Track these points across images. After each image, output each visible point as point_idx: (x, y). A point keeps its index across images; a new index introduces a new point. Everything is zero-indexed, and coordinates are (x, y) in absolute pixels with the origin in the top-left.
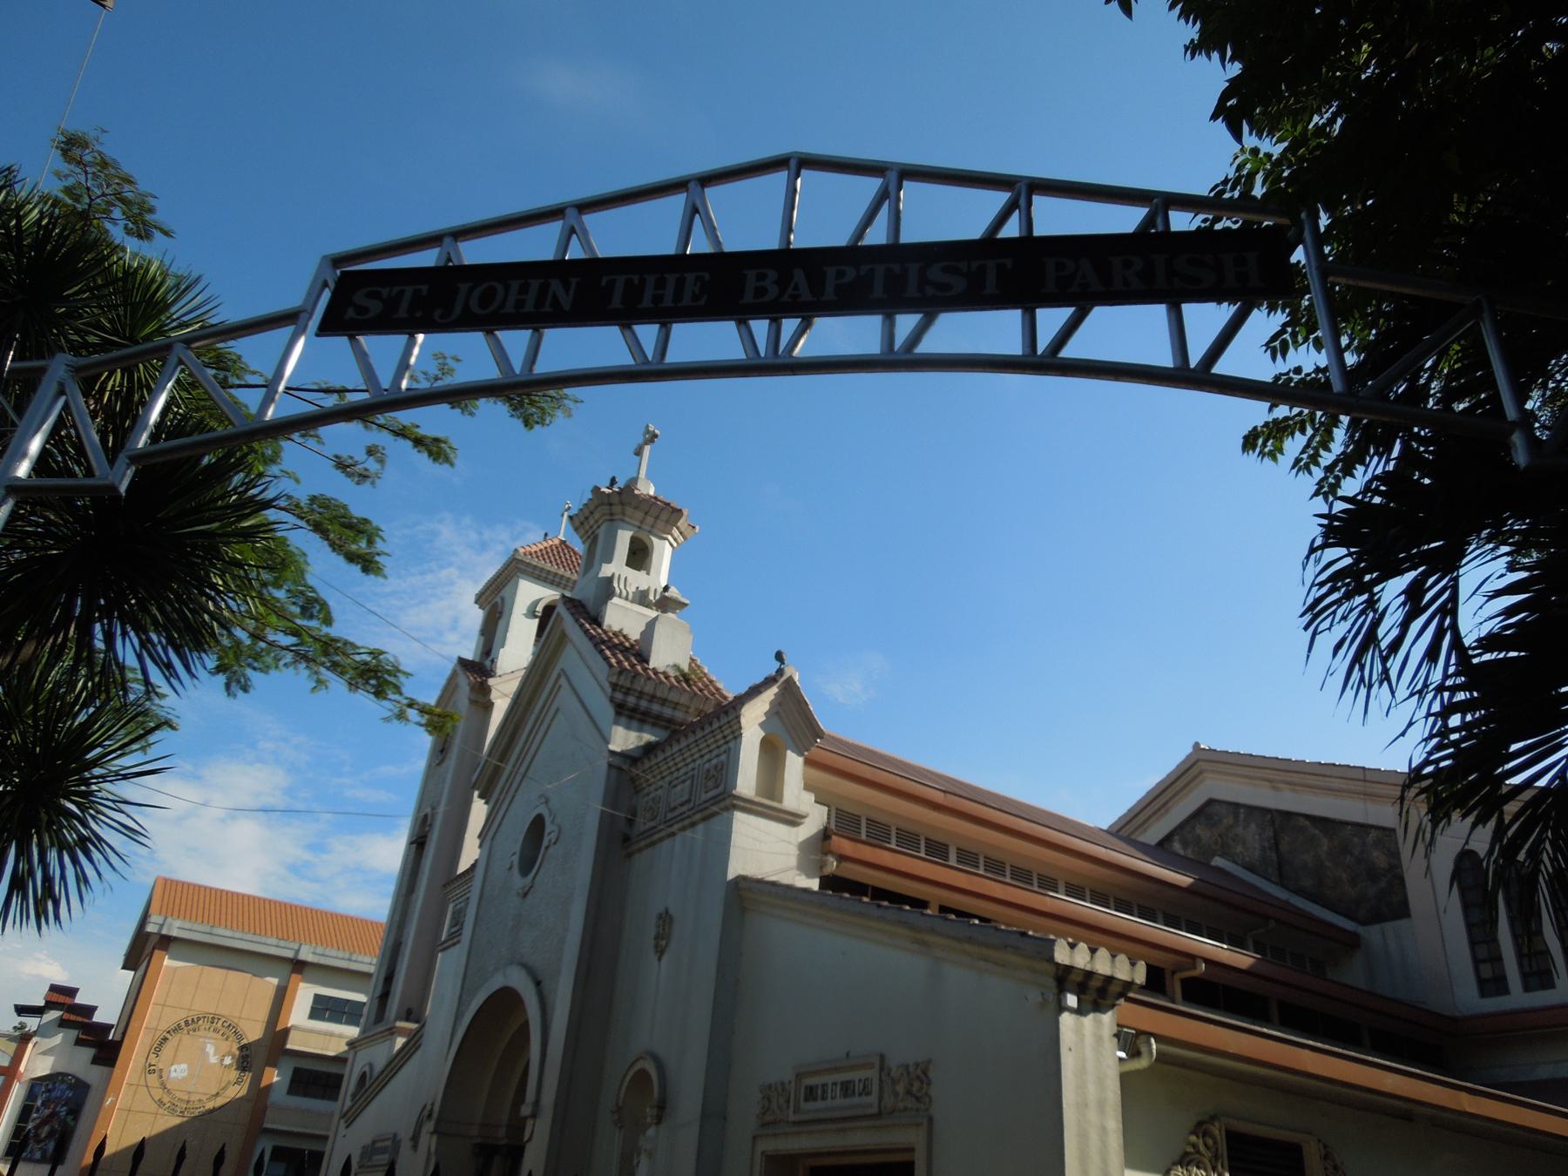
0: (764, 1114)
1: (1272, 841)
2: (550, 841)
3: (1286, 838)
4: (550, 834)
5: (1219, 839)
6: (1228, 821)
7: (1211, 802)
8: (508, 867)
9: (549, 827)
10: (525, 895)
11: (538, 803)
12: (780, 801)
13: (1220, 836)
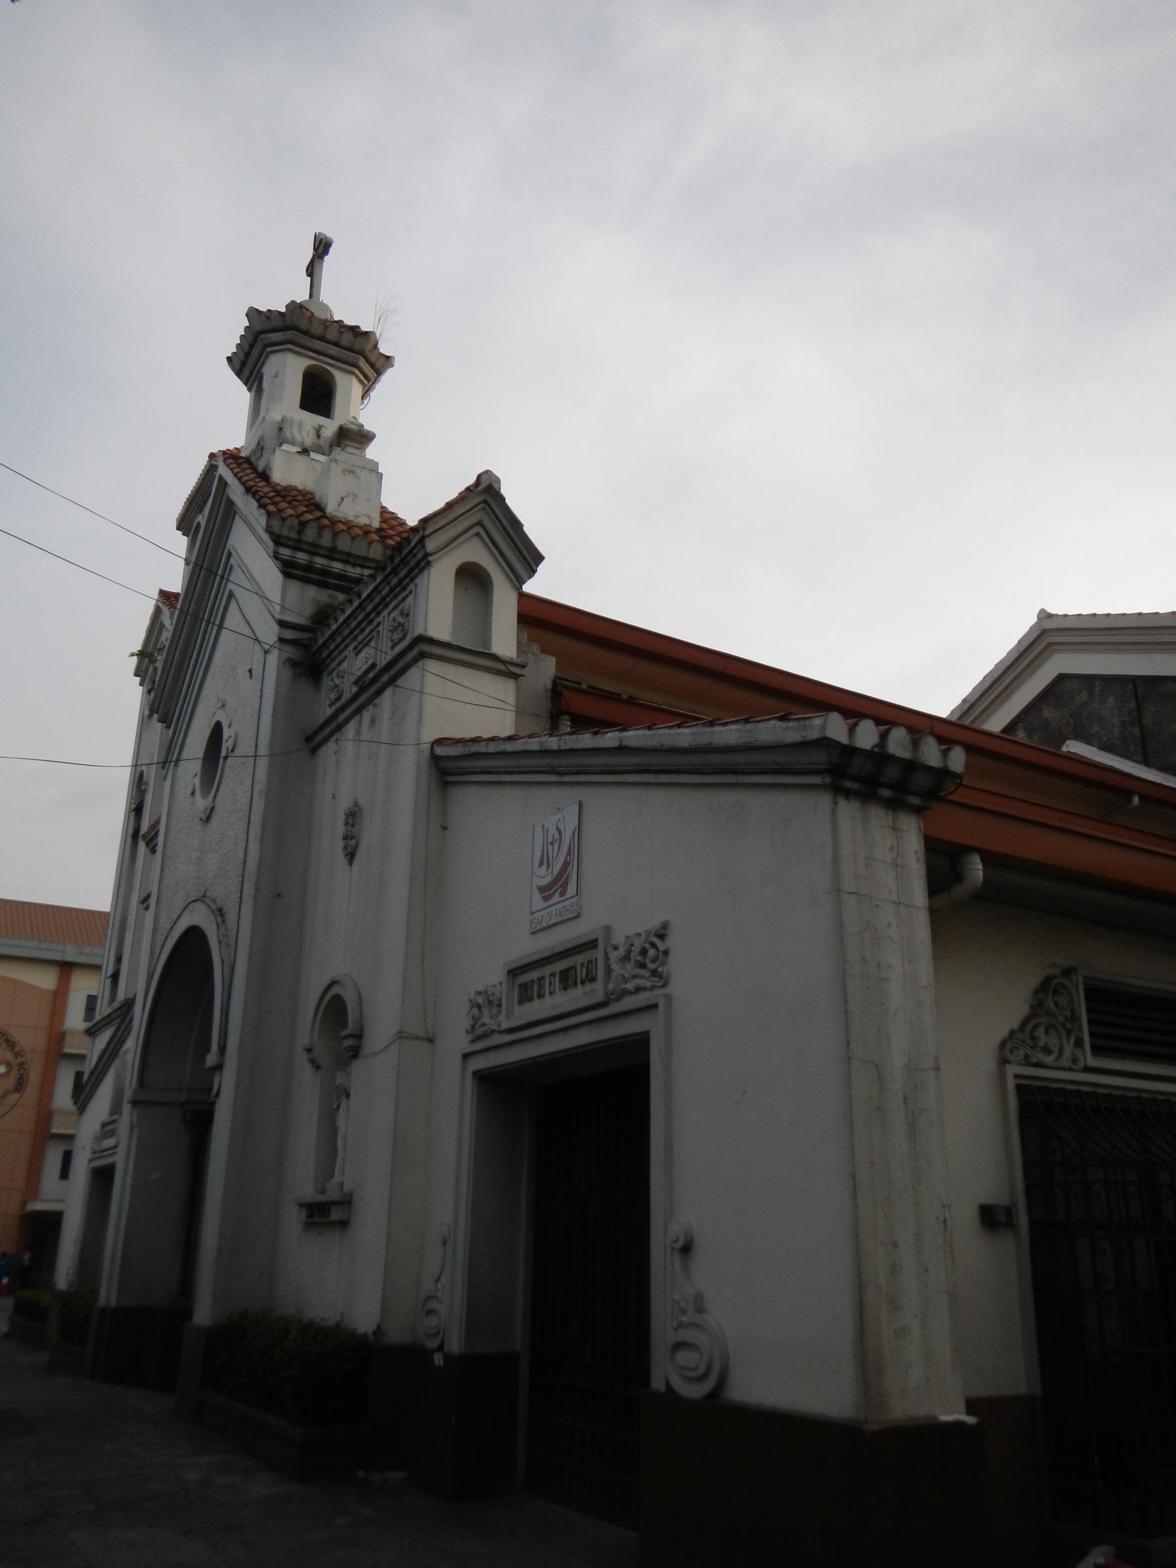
0: (473, 1027)
1: (1135, 714)
2: (228, 749)
3: (1153, 709)
4: (226, 741)
5: (1070, 719)
6: (1083, 696)
7: (1061, 678)
8: (190, 792)
9: (227, 733)
10: (208, 818)
11: (216, 710)
12: (490, 648)
13: (1072, 716)
